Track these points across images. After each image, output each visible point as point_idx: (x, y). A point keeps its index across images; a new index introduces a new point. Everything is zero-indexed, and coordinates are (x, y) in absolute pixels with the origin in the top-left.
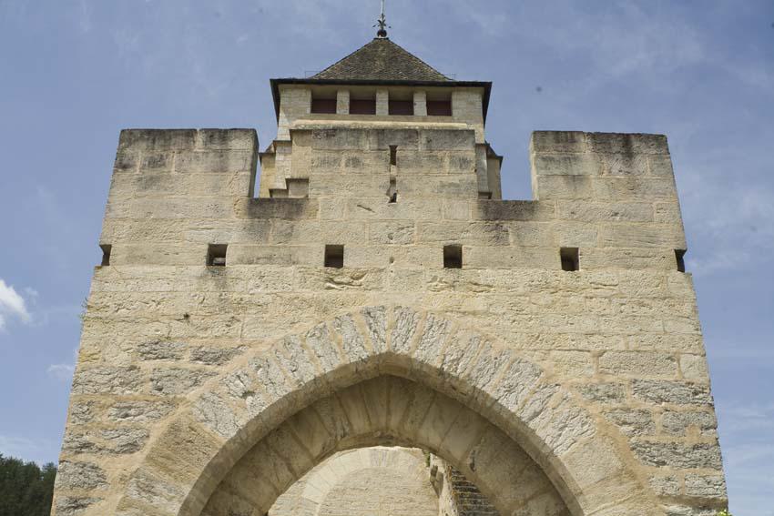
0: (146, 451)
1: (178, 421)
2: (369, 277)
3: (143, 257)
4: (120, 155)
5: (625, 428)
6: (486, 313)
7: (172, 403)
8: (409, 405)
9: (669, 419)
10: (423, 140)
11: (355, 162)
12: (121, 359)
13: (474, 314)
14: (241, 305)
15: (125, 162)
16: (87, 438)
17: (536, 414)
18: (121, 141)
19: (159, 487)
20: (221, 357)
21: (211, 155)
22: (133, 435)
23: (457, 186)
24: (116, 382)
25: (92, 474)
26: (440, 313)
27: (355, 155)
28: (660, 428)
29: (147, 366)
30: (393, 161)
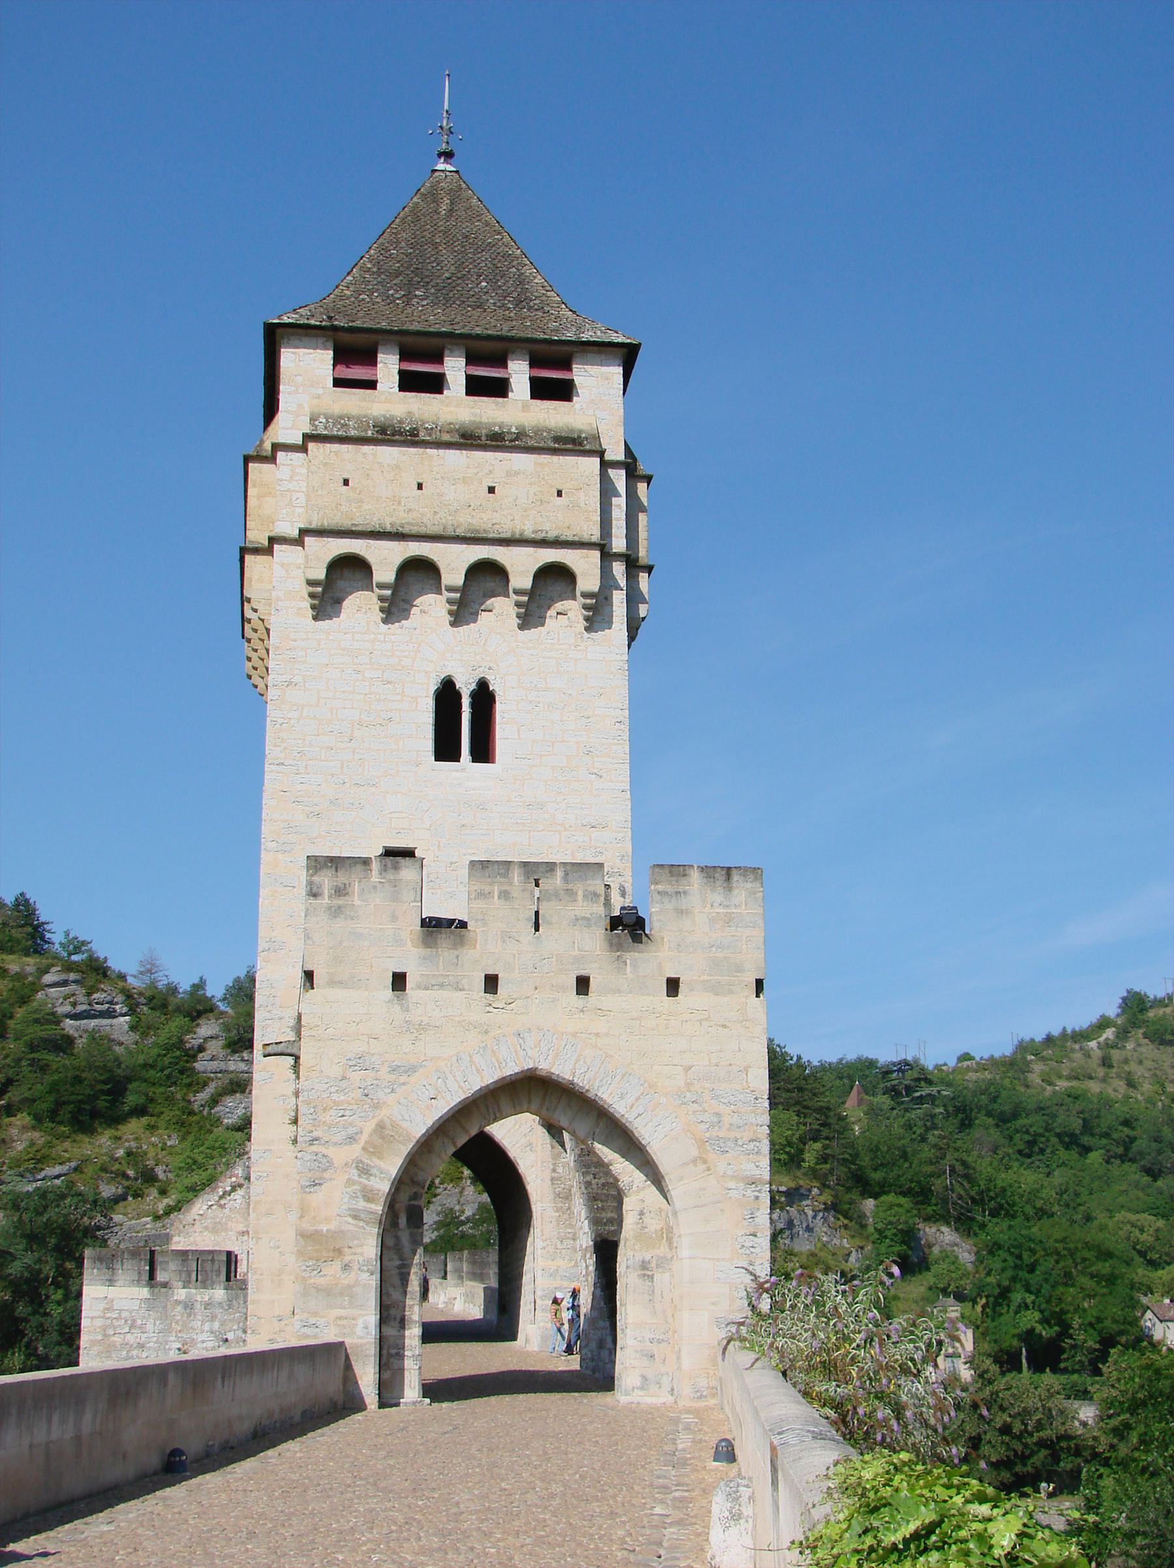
0: (362, 1143)
1: (382, 1121)
2: (518, 1003)
3: (341, 983)
4: (310, 883)
5: (703, 1127)
6: (607, 1035)
7: (377, 1106)
8: (544, 1099)
9: (735, 1120)
10: (559, 873)
11: (505, 895)
12: (336, 1071)
13: (597, 1035)
14: (422, 1027)
15: (315, 890)
16: (315, 1134)
17: (639, 1115)
18: (308, 868)
19: (374, 1171)
20: (412, 1070)
21: (386, 885)
22: (351, 1131)
23: (588, 919)
24: (333, 1089)
25: (325, 1160)
26: (574, 1035)
27: (506, 888)
28: (727, 1126)
29: (355, 1076)
30: (537, 885)
